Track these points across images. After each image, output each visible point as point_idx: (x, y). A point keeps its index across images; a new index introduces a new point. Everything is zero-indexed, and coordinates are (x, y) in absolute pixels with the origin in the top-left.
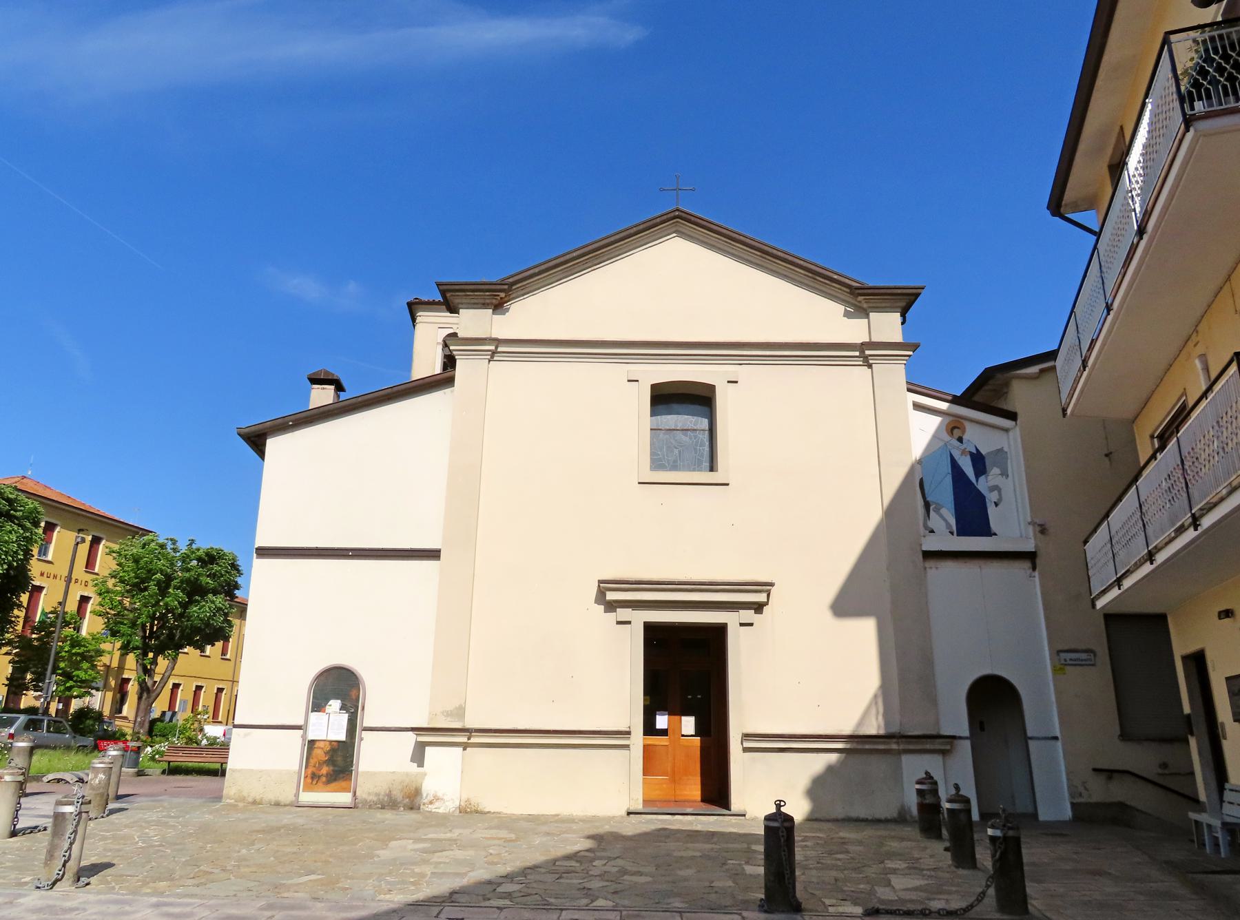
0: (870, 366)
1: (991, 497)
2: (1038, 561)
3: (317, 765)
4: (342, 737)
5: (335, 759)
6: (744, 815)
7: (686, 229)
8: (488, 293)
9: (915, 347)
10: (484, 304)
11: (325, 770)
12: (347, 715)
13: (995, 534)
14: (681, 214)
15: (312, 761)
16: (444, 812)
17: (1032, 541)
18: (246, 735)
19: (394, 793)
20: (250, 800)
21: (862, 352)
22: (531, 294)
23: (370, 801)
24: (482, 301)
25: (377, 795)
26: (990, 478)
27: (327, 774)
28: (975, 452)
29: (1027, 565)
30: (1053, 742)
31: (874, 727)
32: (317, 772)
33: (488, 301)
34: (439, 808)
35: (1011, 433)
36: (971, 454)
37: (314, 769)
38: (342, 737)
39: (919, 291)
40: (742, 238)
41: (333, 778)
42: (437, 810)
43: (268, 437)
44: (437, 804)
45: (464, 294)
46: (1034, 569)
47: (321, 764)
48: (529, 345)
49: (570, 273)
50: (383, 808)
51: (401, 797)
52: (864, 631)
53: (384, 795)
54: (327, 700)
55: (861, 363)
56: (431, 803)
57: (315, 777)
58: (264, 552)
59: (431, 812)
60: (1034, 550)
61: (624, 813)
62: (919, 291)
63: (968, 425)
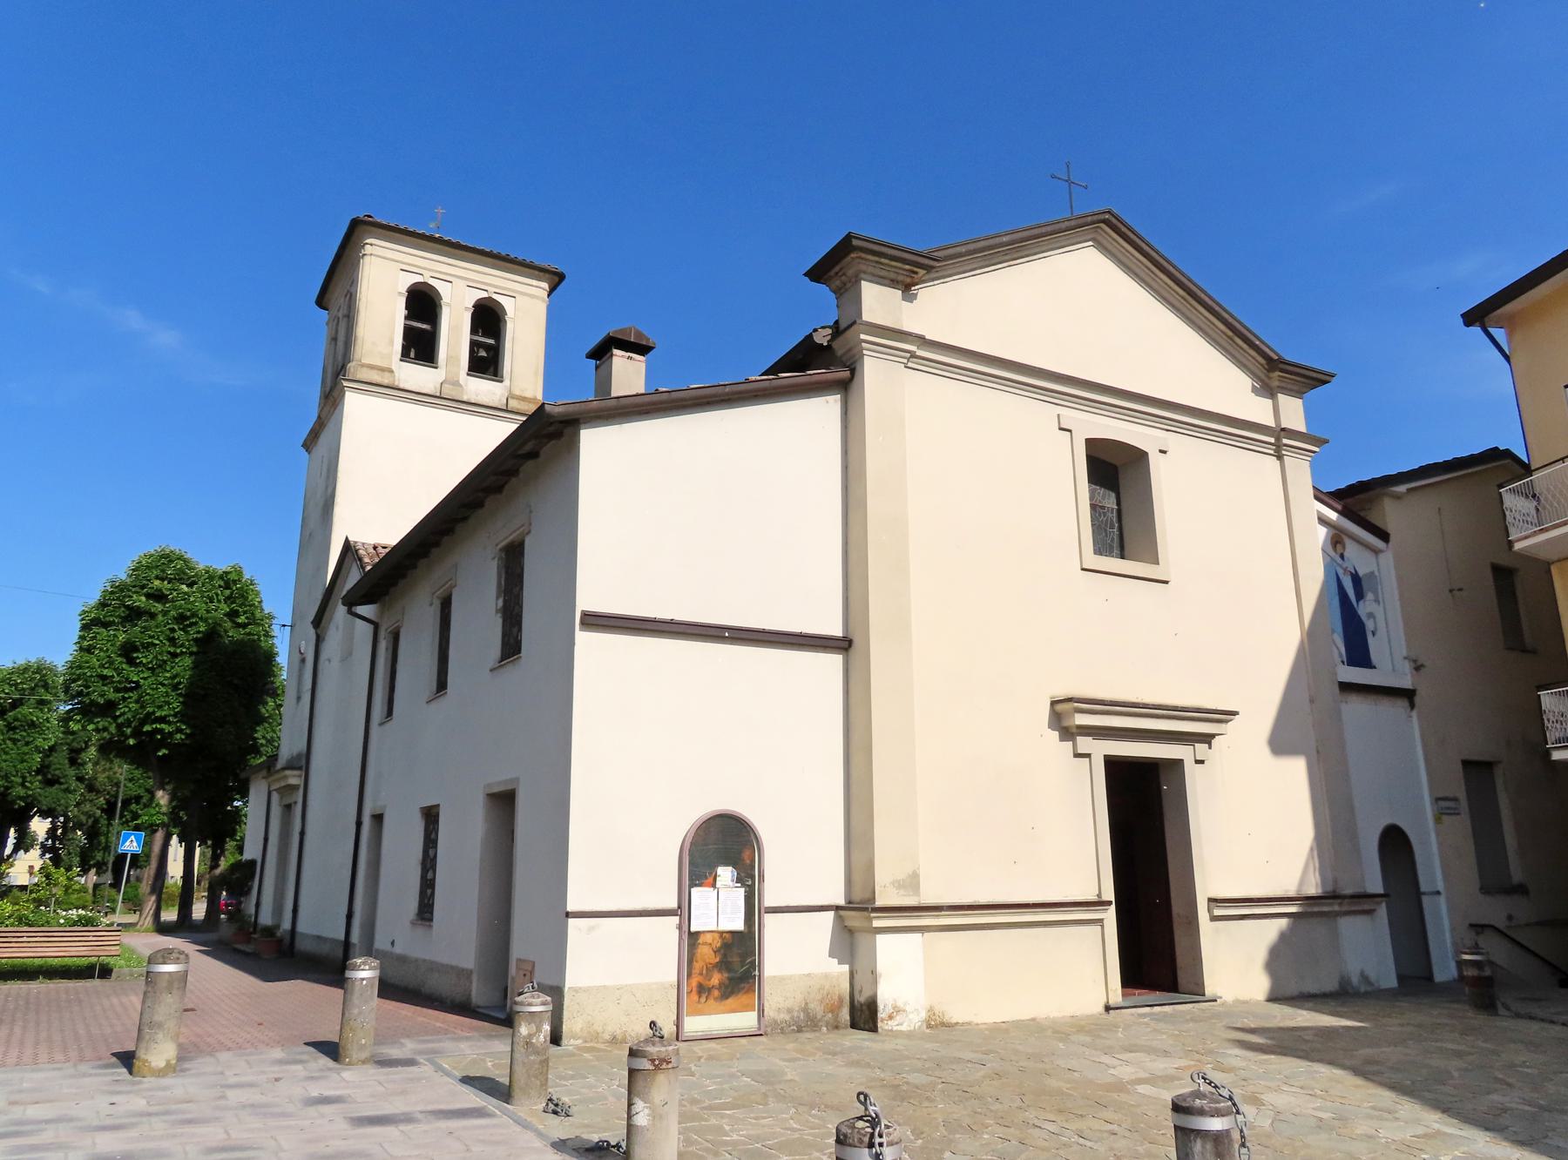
0: (1280, 457)
1: (1369, 625)
2: (1417, 699)
3: (704, 972)
4: (739, 925)
5: (729, 959)
6: (1216, 1001)
7: (1105, 238)
8: (907, 267)
9: (1320, 442)
10: (892, 280)
11: (716, 979)
12: (743, 890)
13: (1375, 667)
14: (1113, 220)
15: (697, 966)
16: (909, 1029)
17: (1409, 677)
18: (591, 929)
19: (811, 1006)
20: (607, 1037)
21: (1278, 439)
22: (942, 281)
23: (782, 1022)
24: (892, 276)
25: (789, 1011)
26: (1367, 603)
27: (720, 984)
28: (1353, 572)
29: (1401, 705)
30: (1436, 897)
31: (1313, 889)
32: (705, 983)
33: (900, 278)
34: (901, 1025)
35: (1381, 556)
36: (1351, 573)
37: (700, 979)
38: (739, 925)
39: (1327, 378)
40: (1171, 269)
41: (729, 990)
42: (899, 1028)
43: (582, 426)
44: (898, 1019)
45: (877, 259)
46: (1412, 706)
47: (710, 969)
48: (951, 354)
49: (987, 263)
50: (800, 1030)
51: (822, 1013)
52: (1296, 770)
53: (798, 1011)
54: (713, 867)
55: (1272, 452)
56: (891, 1017)
57: (702, 990)
58: (595, 621)
59: (891, 1030)
60: (1411, 687)
61: (1101, 1009)
62: (1327, 378)
63: (1348, 542)
